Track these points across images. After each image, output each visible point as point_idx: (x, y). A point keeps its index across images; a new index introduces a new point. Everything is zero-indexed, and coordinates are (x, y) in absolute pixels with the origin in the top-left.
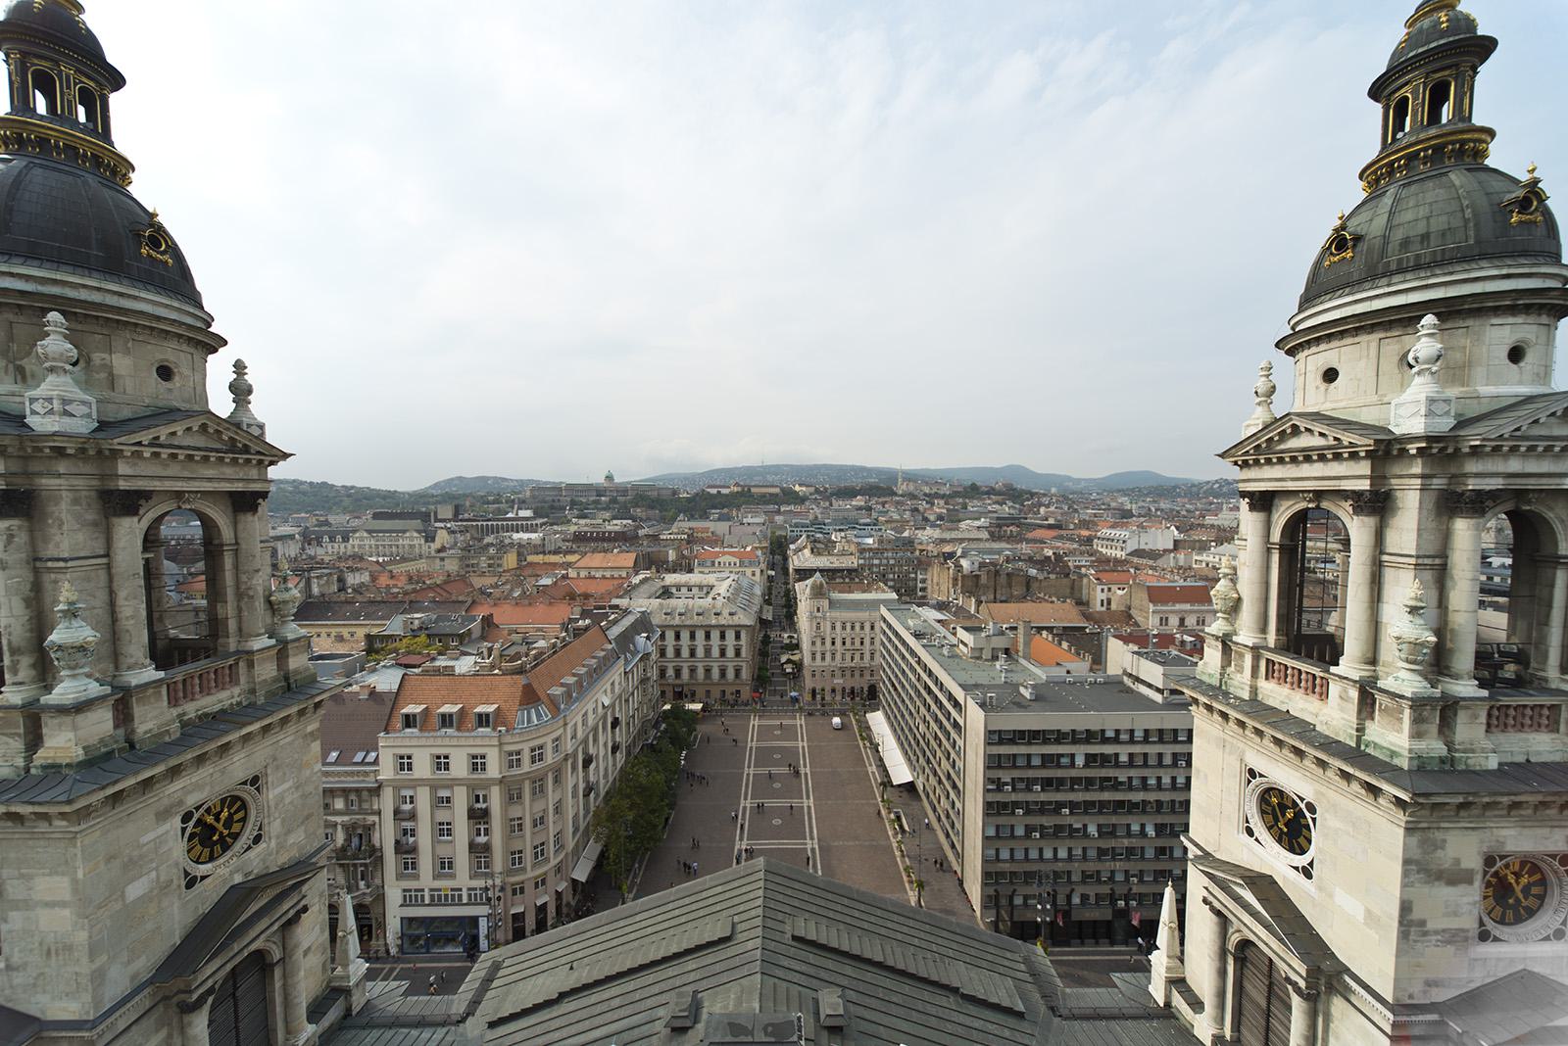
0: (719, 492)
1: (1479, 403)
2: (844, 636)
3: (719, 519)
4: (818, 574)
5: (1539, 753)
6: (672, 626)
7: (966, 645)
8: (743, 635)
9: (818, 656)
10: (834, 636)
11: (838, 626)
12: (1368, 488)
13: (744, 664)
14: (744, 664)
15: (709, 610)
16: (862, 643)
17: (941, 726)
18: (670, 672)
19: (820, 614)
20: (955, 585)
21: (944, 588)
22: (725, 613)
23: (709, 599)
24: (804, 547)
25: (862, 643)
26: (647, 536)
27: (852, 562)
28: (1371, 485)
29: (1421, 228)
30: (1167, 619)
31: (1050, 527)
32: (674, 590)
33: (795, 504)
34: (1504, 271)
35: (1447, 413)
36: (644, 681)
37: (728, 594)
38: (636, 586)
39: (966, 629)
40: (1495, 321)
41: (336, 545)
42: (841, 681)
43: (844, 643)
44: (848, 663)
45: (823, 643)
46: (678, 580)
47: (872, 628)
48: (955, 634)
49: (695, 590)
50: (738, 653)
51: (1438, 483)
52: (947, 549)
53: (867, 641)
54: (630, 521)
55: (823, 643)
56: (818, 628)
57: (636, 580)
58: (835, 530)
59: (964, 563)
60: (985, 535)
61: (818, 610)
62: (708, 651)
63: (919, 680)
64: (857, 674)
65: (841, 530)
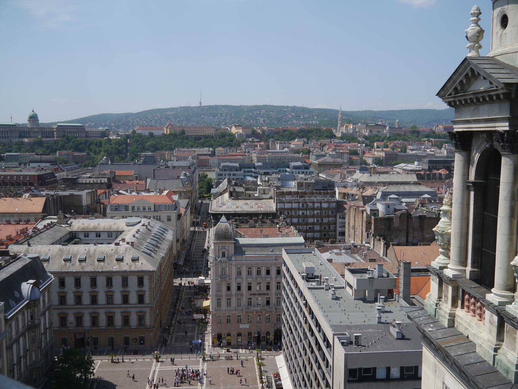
0: (151, 135)
2: (250, 280)
3: (145, 163)
4: (223, 219)
6: (72, 272)
7: (351, 287)
10: (239, 280)
12: (507, 129)
14: (148, 310)
15: (111, 256)
16: (268, 288)
17: (319, 367)
18: (71, 319)
20: (368, 228)
21: (358, 232)
22: (128, 259)
23: (113, 246)
24: (225, 191)
25: (268, 288)
26: (65, 180)
27: (271, 206)
28: (510, 126)
32: (82, 236)
36: (32, 327)
37: (134, 240)
38: (37, 232)
39: (353, 272)
42: (247, 326)
46: (86, 225)
48: (343, 276)
49: (104, 236)
50: (141, 299)
52: (369, 192)
53: (273, 286)
54: (48, 165)
57: (40, 226)
58: (261, 175)
59: (380, 207)
60: (413, 178)
61: (224, 255)
62: (110, 298)
63: (306, 323)
65: (266, 174)
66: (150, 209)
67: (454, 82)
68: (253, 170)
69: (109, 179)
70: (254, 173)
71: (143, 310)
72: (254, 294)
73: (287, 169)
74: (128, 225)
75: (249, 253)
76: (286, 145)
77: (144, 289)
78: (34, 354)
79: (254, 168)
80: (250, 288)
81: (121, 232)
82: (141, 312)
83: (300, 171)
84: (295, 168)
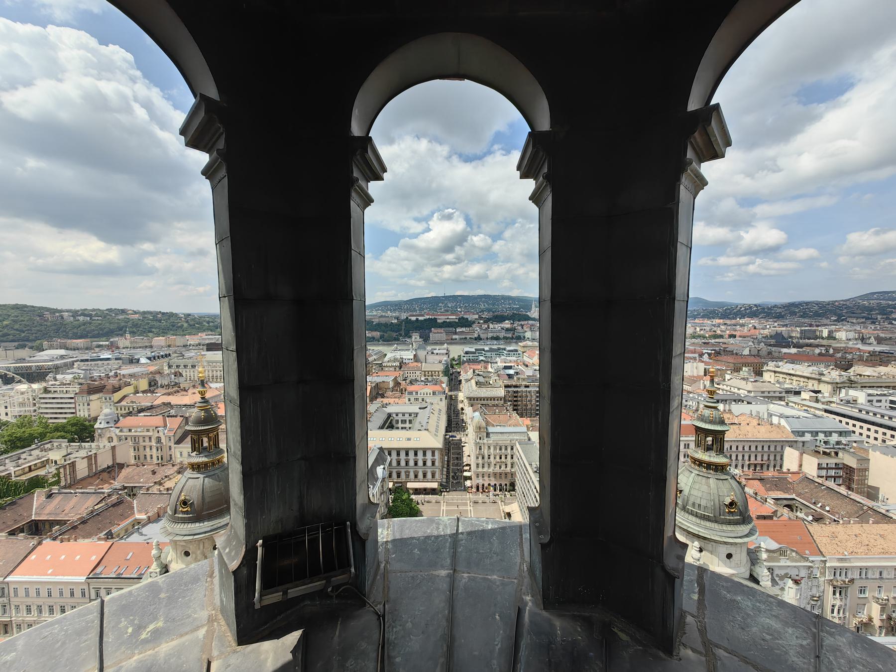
0: (417, 319)
2: (495, 454)
8: (437, 453)
9: (481, 465)
11: (492, 448)
13: (437, 470)
14: (437, 470)
16: (506, 458)
19: (481, 441)
24: (471, 379)
25: (506, 458)
30: (688, 445)
33: (466, 327)
41: (188, 370)
43: (495, 458)
44: (497, 469)
45: (483, 458)
47: (512, 449)
50: (433, 463)
53: (509, 457)
55: (483, 458)
56: (480, 449)
61: (480, 439)
64: (503, 476)
66: (430, 394)
68: (483, 352)
69: (400, 363)
70: (485, 354)
71: (435, 470)
72: (498, 462)
73: (504, 351)
74: (420, 408)
75: (493, 437)
76: (500, 325)
77: (435, 458)
78: (383, 508)
79: (484, 351)
80: (495, 458)
81: (417, 414)
82: (433, 471)
83: (513, 353)
84: (510, 351)
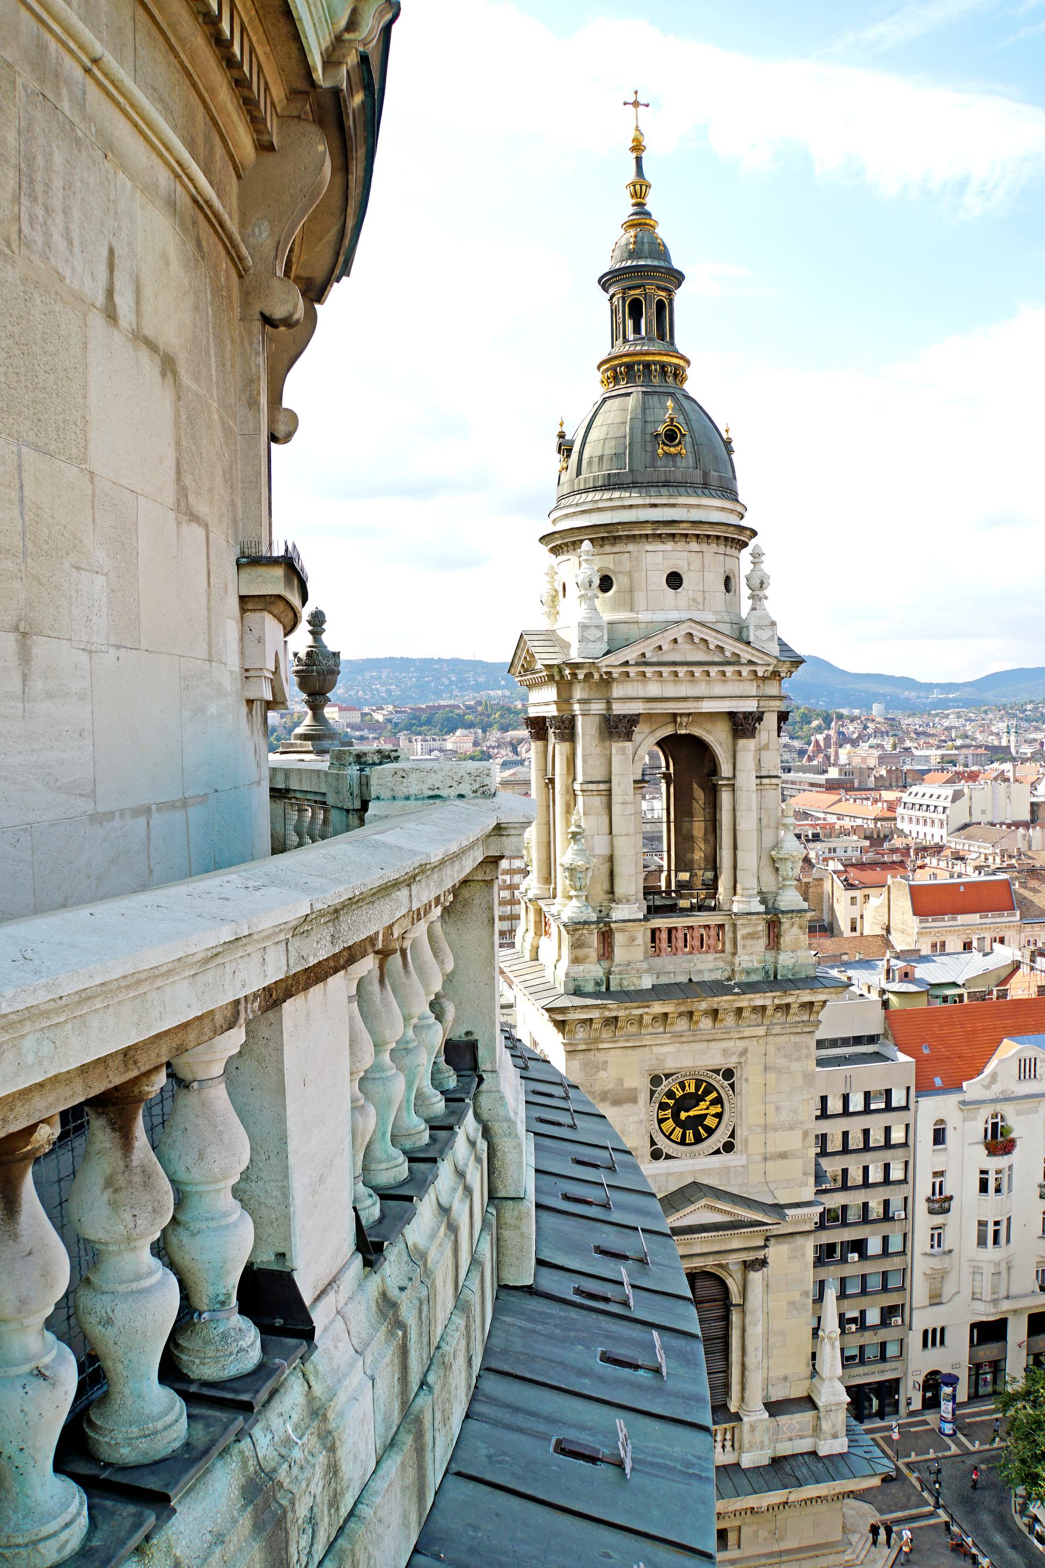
1: (639, 628)
5: (700, 972)
28: (558, 710)
29: (599, 453)
31: (831, 786)
34: (648, 501)
35: (600, 639)
40: (649, 547)
51: (598, 707)
67: (520, 658)
